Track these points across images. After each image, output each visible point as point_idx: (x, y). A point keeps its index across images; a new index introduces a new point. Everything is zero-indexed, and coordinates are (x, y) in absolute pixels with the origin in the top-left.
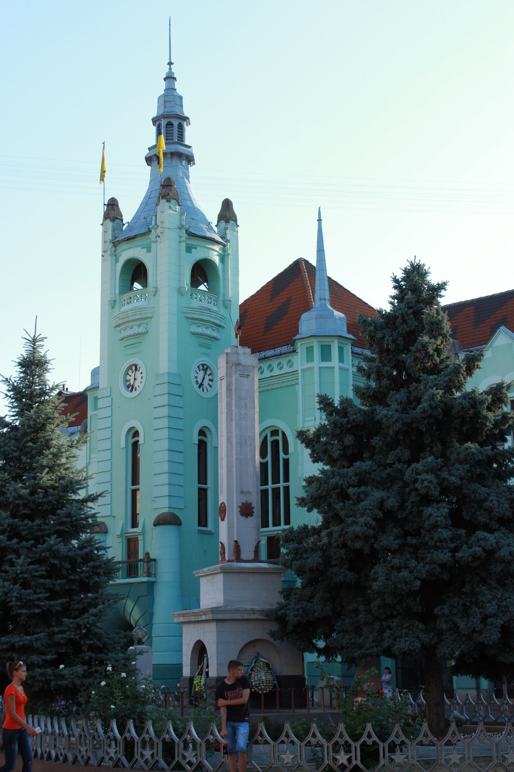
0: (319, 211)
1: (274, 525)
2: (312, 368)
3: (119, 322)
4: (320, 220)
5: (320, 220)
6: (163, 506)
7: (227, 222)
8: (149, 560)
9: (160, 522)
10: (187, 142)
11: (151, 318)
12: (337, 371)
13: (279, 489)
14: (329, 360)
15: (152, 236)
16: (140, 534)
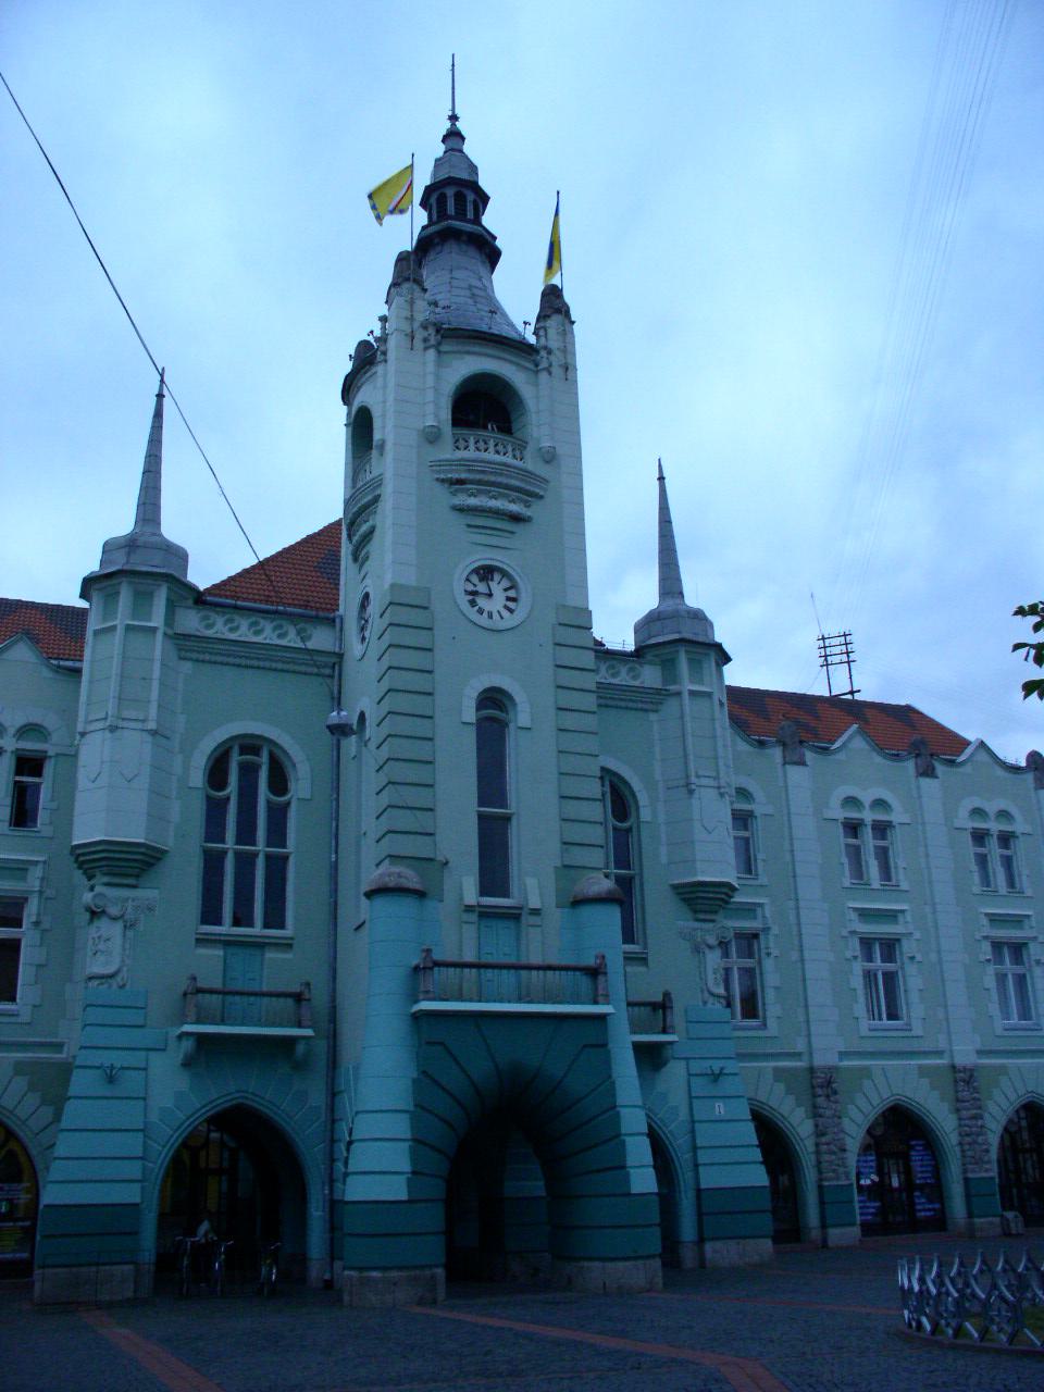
0: (660, 465)
2: (709, 695)
3: (463, 476)
4: (661, 478)
5: (661, 478)
11: (542, 497)
16: (536, 912)
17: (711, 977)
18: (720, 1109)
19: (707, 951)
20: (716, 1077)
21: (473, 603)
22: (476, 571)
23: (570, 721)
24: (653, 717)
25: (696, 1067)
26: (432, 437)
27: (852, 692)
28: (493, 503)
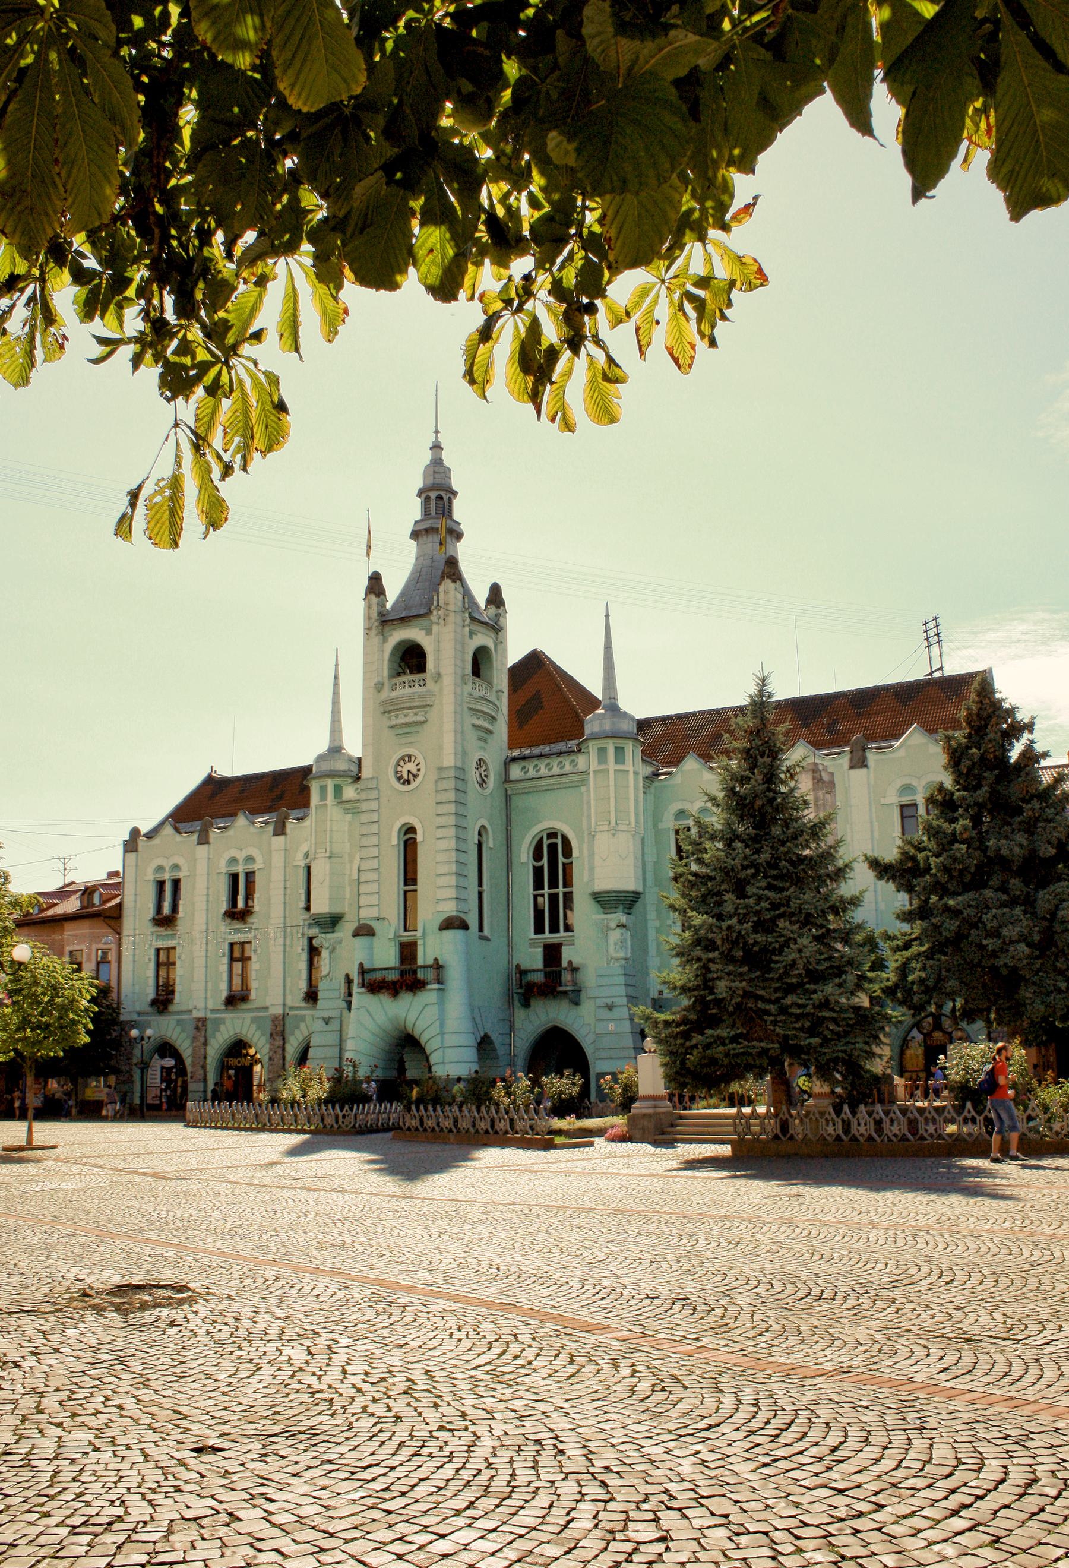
1: (551, 932)
4: (607, 616)
5: (607, 616)
6: (449, 909)
7: (498, 607)
8: (438, 966)
9: (448, 924)
10: (455, 517)
12: (631, 775)
13: (557, 894)
14: (623, 763)
15: (433, 618)
17: (611, 948)
18: (612, 1027)
19: (611, 933)
20: (610, 1008)
21: (399, 779)
22: (403, 758)
23: (440, 833)
24: (583, 789)
25: (600, 1002)
26: (379, 687)
27: (941, 668)
28: (402, 720)
